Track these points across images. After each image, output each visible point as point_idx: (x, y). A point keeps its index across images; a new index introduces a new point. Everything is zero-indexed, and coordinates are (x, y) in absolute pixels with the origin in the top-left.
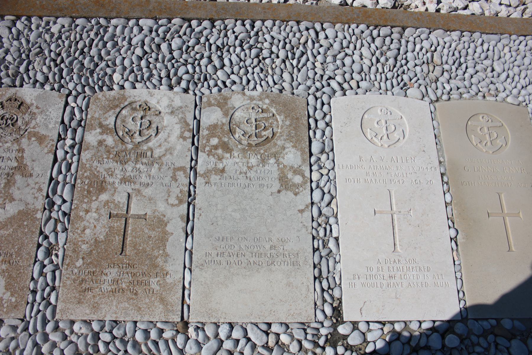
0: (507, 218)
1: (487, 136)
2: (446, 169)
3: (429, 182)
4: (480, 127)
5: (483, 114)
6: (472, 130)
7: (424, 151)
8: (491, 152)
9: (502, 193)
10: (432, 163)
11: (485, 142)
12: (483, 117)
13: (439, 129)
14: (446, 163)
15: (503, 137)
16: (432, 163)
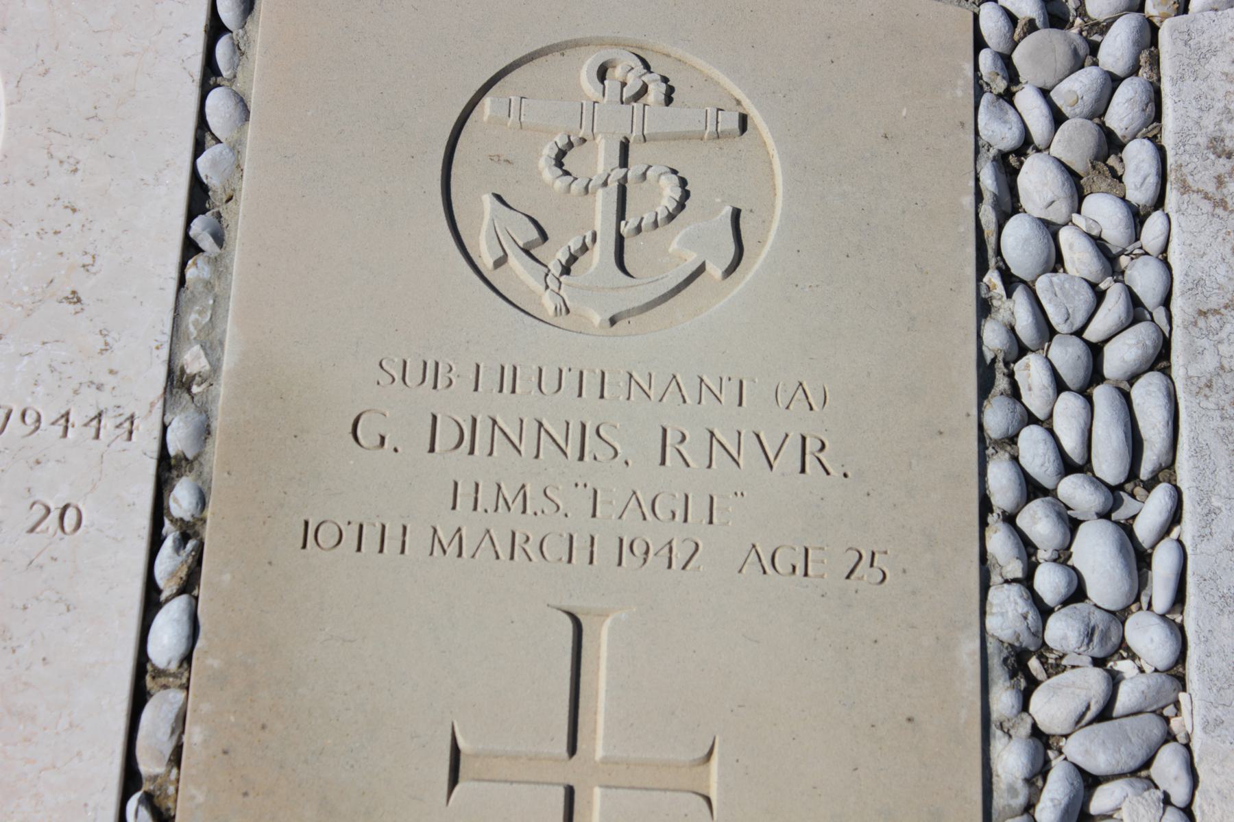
0: (597, 791)
1: (604, 202)
2: (205, 432)
3: (55, 514)
4: (562, 142)
6: (496, 159)
7: (75, 298)
8: (597, 318)
9: (603, 615)
10: (110, 381)
11: (575, 245)
12: (602, 74)
13: (236, 149)
14: (222, 389)
15: (727, 211)
16: (110, 381)
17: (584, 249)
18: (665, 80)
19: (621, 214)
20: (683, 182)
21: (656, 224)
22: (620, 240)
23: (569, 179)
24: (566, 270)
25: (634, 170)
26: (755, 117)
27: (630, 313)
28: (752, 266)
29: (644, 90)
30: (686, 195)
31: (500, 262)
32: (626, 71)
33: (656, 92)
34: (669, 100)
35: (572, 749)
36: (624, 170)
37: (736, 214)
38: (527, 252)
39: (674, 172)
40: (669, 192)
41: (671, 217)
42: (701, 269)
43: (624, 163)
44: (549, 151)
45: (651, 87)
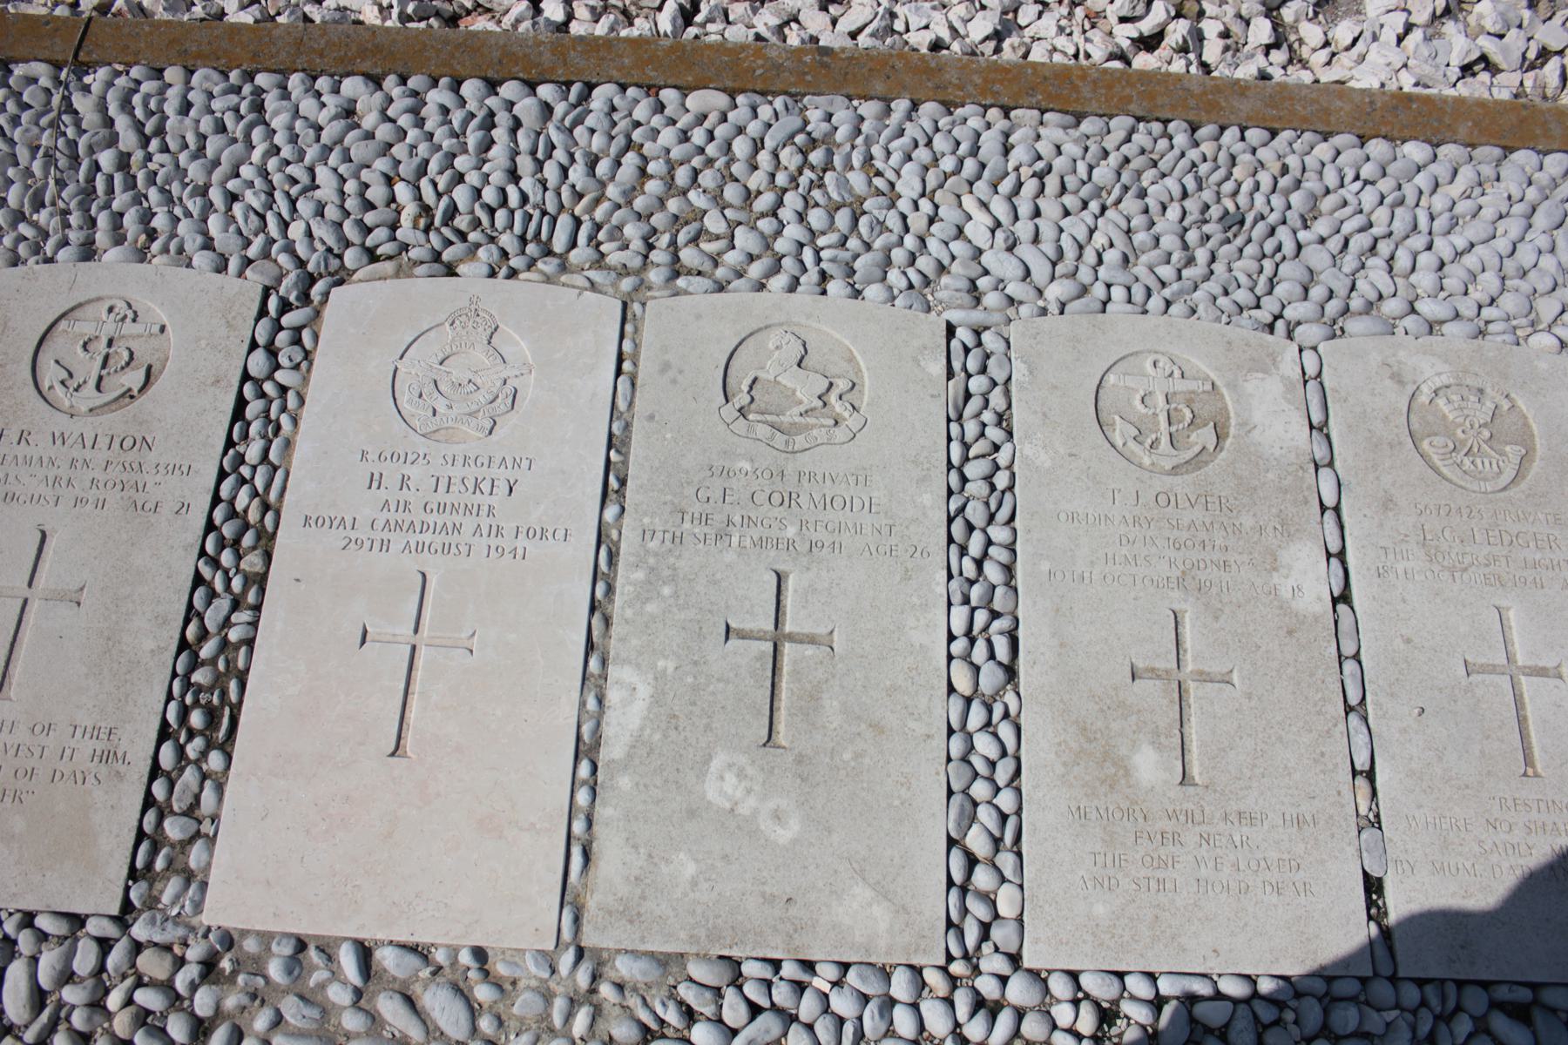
1: (99, 360)
8: (84, 409)
11: (81, 381)
17: (85, 382)
18: (135, 313)
19: (104, 365)
22: (100, 378)
24: (76, 390)
25: (112, 350)
26: (169, 328)
27: (96, 408)
29: (125, 317)
31: (51, 388)
32: (121, 307)
33: (130, 315)
34: (134, 320)
35: (30, 585)
37: (149, 368)
40: (126, 355)
41: (122, 368)
44: (81, 343)
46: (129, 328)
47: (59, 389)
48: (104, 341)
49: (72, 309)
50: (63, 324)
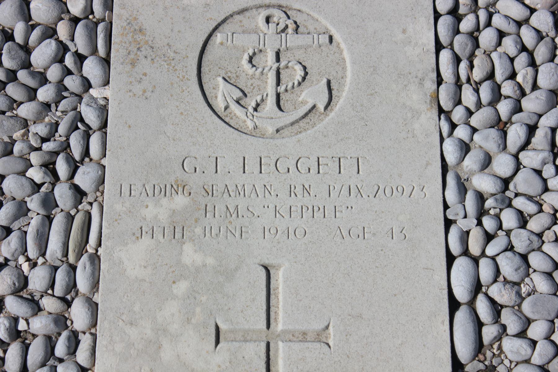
4: (251, 52)
5: (268, 6)
8: (271, 130)
11: (259, 98)
15: (325, 81)
18: (295, 23)
19: (278, 83)
20: (305, 68)
21: (293, 87)
22: (278, 96)
23: (254, 68)
25: (283, 64)
26: (337, 37)
28: (340, 103)
30: (306, 74)
31: (226, 108)
33: (291, 26)
36: (278, 64)
38: (238, 102)
39: (300, 63)
40: (300, 72)
42: (314, 107)
43: (278, 59)
44: (246, 57)
45: (289, 25)
46: (292, 39)
47: (234, 107)
48: (271, 57)
49: (224, 21)
50: (219, 37)
